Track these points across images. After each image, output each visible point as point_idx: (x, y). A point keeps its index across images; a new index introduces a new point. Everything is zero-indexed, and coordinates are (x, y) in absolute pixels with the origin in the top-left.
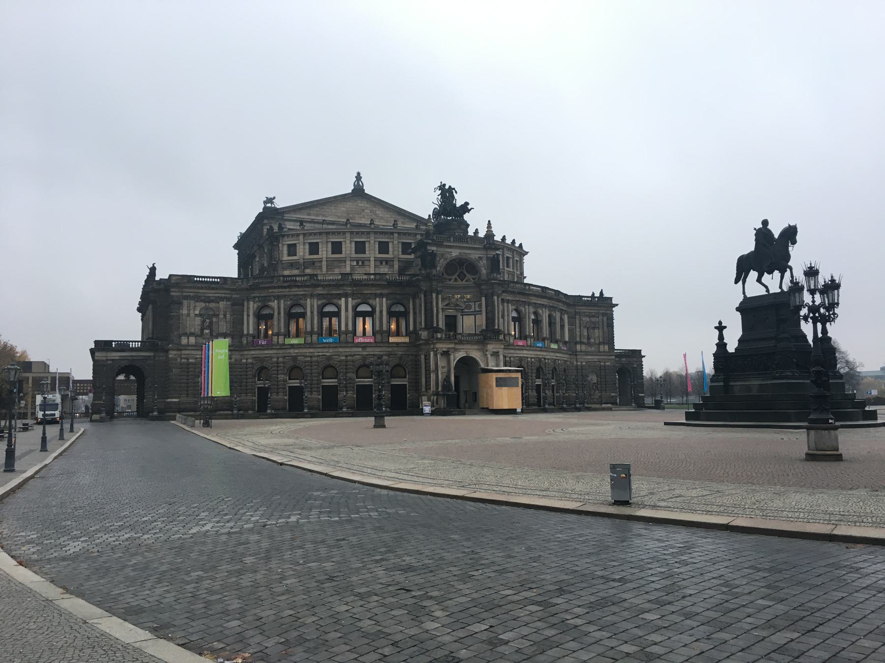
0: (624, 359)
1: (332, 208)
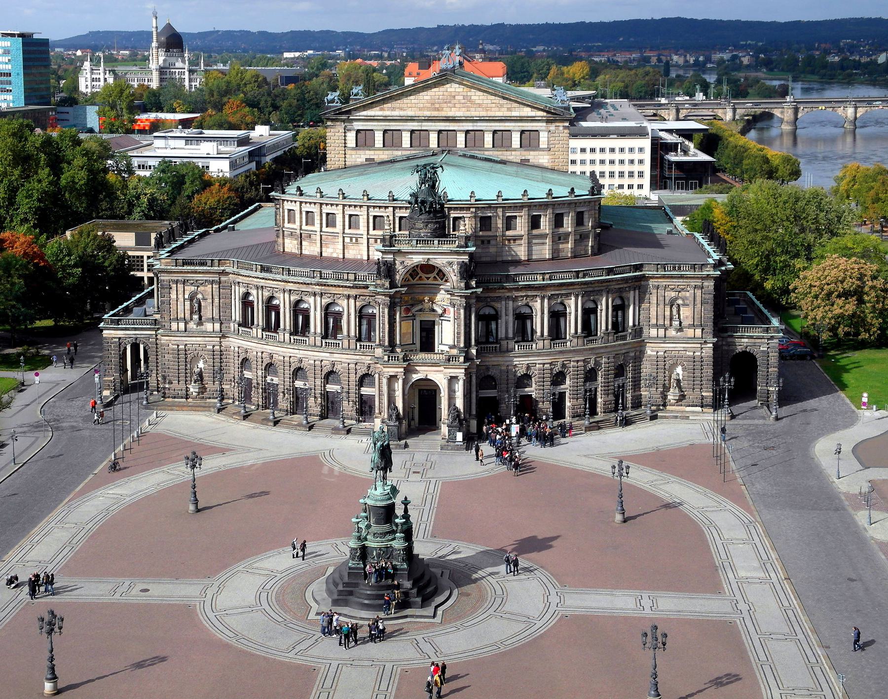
0: (746, 340)
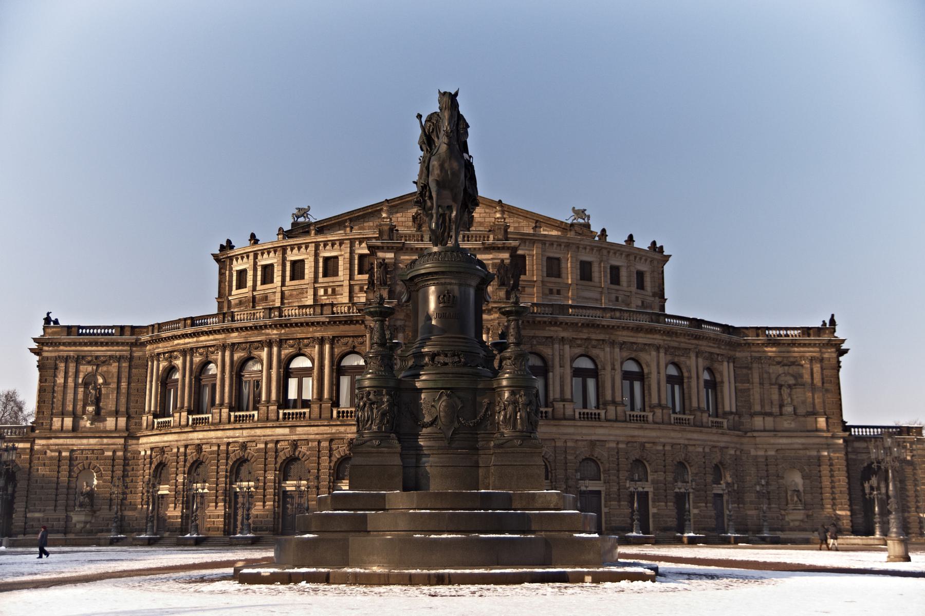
1: (399, 215)
